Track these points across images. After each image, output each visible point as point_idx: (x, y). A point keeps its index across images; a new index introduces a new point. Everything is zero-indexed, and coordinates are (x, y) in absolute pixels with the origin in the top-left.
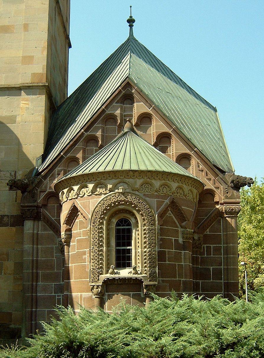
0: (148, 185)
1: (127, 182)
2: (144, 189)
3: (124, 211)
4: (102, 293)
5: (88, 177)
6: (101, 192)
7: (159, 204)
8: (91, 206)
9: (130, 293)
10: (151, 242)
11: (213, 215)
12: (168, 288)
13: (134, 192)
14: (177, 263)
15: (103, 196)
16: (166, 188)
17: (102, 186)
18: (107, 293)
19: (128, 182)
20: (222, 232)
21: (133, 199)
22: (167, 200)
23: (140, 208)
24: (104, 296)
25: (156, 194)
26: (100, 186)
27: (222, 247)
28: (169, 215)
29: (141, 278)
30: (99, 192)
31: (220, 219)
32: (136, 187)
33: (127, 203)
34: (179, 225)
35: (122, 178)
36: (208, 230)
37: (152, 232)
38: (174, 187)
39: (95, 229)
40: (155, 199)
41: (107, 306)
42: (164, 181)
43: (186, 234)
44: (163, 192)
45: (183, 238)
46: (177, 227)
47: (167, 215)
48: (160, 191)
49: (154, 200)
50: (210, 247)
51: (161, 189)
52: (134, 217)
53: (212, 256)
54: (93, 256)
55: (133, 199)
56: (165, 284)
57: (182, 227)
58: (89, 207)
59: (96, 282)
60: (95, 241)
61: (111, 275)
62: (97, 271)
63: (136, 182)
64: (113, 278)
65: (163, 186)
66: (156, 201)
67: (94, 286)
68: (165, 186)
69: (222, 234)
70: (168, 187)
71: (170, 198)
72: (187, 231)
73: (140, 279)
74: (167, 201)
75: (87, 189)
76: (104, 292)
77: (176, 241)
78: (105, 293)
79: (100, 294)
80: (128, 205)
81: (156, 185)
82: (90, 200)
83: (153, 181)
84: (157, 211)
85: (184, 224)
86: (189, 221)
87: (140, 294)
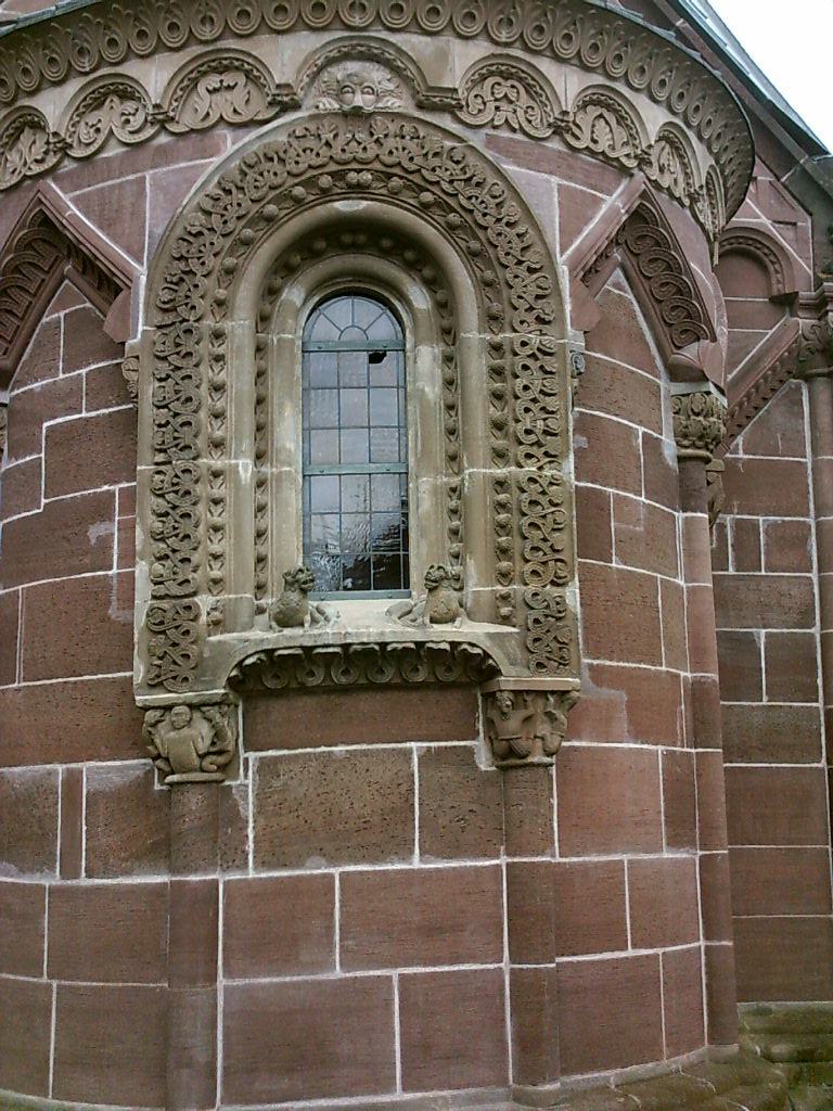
0: (513, 87)
1: (390, 54)
2: (491, 105)
3: (362, 238)
4: (220, 753)
5: (137, 19)
6: (221, 117)
7: (576, 211)
8: (153, 209)
9: (408, 745)
10: (540, 424)
11: (768, 363)
12: (624, 715)
13: (428, 117)
14: (659, 576)
15: (231, 144)
16: (607, 123)
17: (228, 79)
18: (252, 756)
19: (399, 50)
20: (808, 450)
21: (426, 155)
22: (614, 195)
23: (468, 218)
24: (236, 777)
25: (555, 144)
26: (213, 81)
27: (813, 530)
28: (617, 292)
29: (486, 645)
30: (208, 114)
31: (798, 388)
32: (447, 84)
33: (390, 176)
34: (659, 362)
35: (357, 21)
36: (740, 440)
37: (542, 367)
38: (649, 127)
39: (178, 345)
40: (551, 173)
41: (251, 837)
42: (600, 80)
43: (698, 414)
44: (595, 142)
45: (682, 435)
46: (653, 370)
47: (606, 286)
48: (577, 131)
49: (549, 181)
50: (755, 525)
51: (585, 120)
52: (427, 272)
53: (763, 573)
54: (166, 514)
55: (426, 155)
56: (607, 693)
57: (676, 373)
58: (138, 214)
59: (186, 679)
60: (176, 415)
61: (287, 631)
62: (188, 608)
63: (443, 56)
64: (302, 647)
65: (593, 111)
66: (559, 191)
67: (168, 708)
68: (606, 114)
69: (808, 460)
70: (621, 120)
71: (626, 187)
72: (708, 393)
73: (476, 651)
74: (614, 203)
75: (130, 106)
76: (237, 744)
77: (652, 444)
78: (243, 755)
79: (206, 763)
80: (394, 193)
81: (560, 90)
82: (148, 175)
83: (546, 66)
84: (562, 252)
85: (690, 353)
86: (714, 339)
87: (470, 751)
